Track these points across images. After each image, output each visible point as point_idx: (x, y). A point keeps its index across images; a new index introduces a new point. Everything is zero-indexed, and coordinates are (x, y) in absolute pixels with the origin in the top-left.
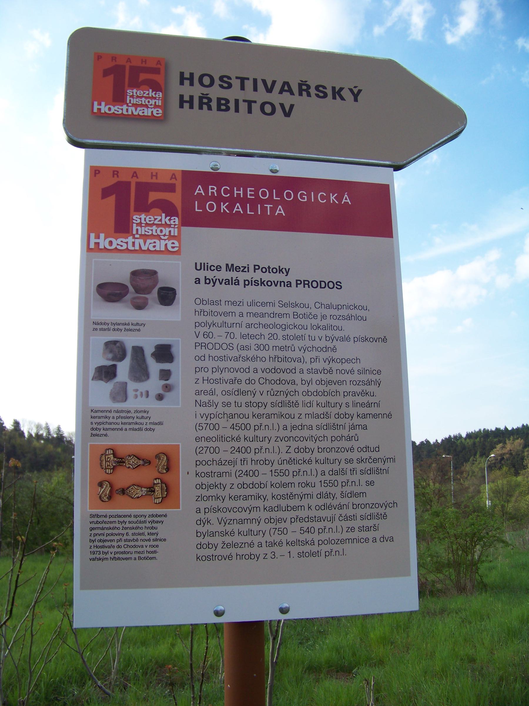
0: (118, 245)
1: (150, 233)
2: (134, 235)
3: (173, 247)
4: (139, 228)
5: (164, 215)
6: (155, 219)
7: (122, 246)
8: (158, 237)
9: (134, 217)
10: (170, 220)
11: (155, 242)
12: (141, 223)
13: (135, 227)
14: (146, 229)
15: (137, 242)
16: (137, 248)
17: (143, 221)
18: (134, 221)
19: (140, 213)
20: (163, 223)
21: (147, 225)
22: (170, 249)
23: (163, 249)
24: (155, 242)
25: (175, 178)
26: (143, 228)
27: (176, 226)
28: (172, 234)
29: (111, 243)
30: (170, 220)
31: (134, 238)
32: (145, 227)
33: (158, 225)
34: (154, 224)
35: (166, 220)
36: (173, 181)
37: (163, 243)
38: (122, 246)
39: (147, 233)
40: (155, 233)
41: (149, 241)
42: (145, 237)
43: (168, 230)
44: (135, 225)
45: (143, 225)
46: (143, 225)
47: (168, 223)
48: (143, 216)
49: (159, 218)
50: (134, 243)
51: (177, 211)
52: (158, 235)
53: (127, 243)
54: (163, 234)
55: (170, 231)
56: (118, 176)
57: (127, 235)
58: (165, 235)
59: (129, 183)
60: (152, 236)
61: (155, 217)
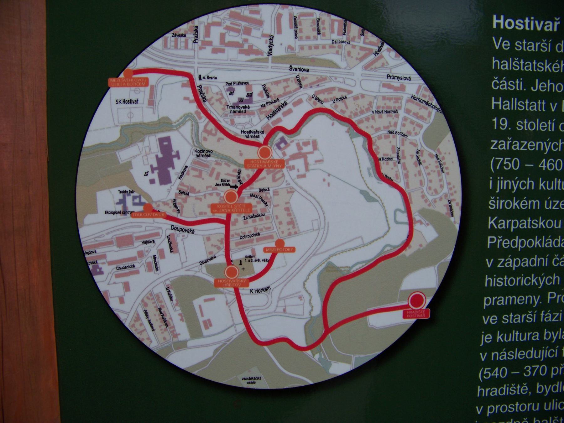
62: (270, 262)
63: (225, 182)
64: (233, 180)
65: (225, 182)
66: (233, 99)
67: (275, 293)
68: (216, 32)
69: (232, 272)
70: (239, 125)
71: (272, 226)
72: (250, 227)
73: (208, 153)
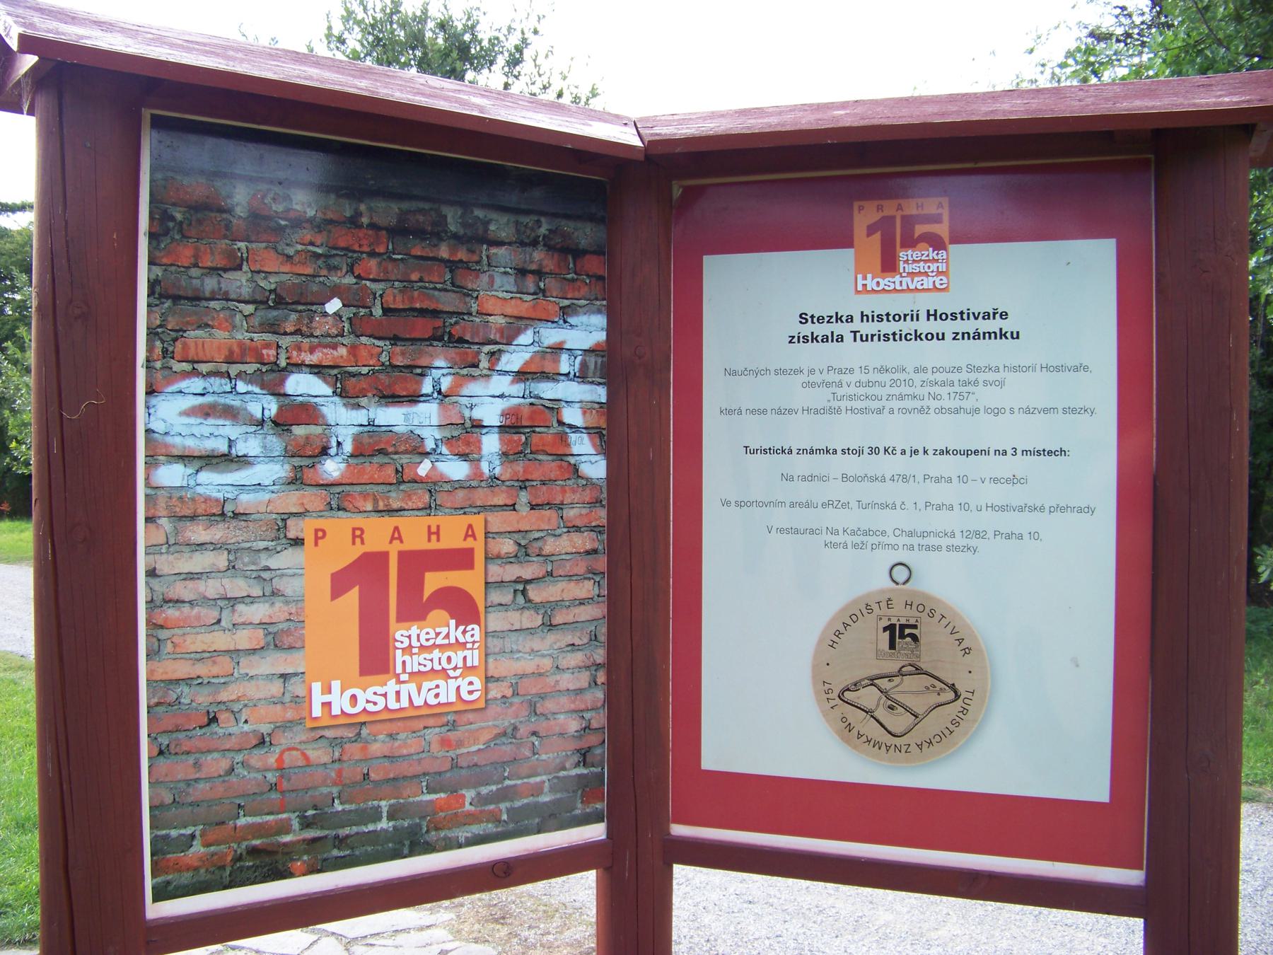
0: (368, 701)
3: (470, 692)
4: (407, 658)
5: (452, 623)
6: (438, 634)
7: (375, 704)
9: (398, 636)
10: (464, 632)
11: (437, 686)
12: (410, 646)
17: (415, 643)
18: (398, 645)
19: (407, 624)
23: (453, 698)
24: (437, 686)
25: (474, 536)
27: (476, 645)
28: (469, 664)
30: (464, 632)
31: (399, 682)
32: (419, 654)
34: (435, 646)
35: (456, 633)
36: (470, 543)
37: (453, 684)
38: (375, 704)
39: (422, 669)
40: (437, 667)
41: (426, 685)
43: (461, 654)
44: (399, 652)
47: (461, 640)
49: (444, 631)
50: (398, 693)
52: (444, 670)
53: (385, 695)
54: (453, 665)
55: (465, 658)
56: (363, 542)
58: (455, 668)
59: (385, 555)
61: (438, 630)
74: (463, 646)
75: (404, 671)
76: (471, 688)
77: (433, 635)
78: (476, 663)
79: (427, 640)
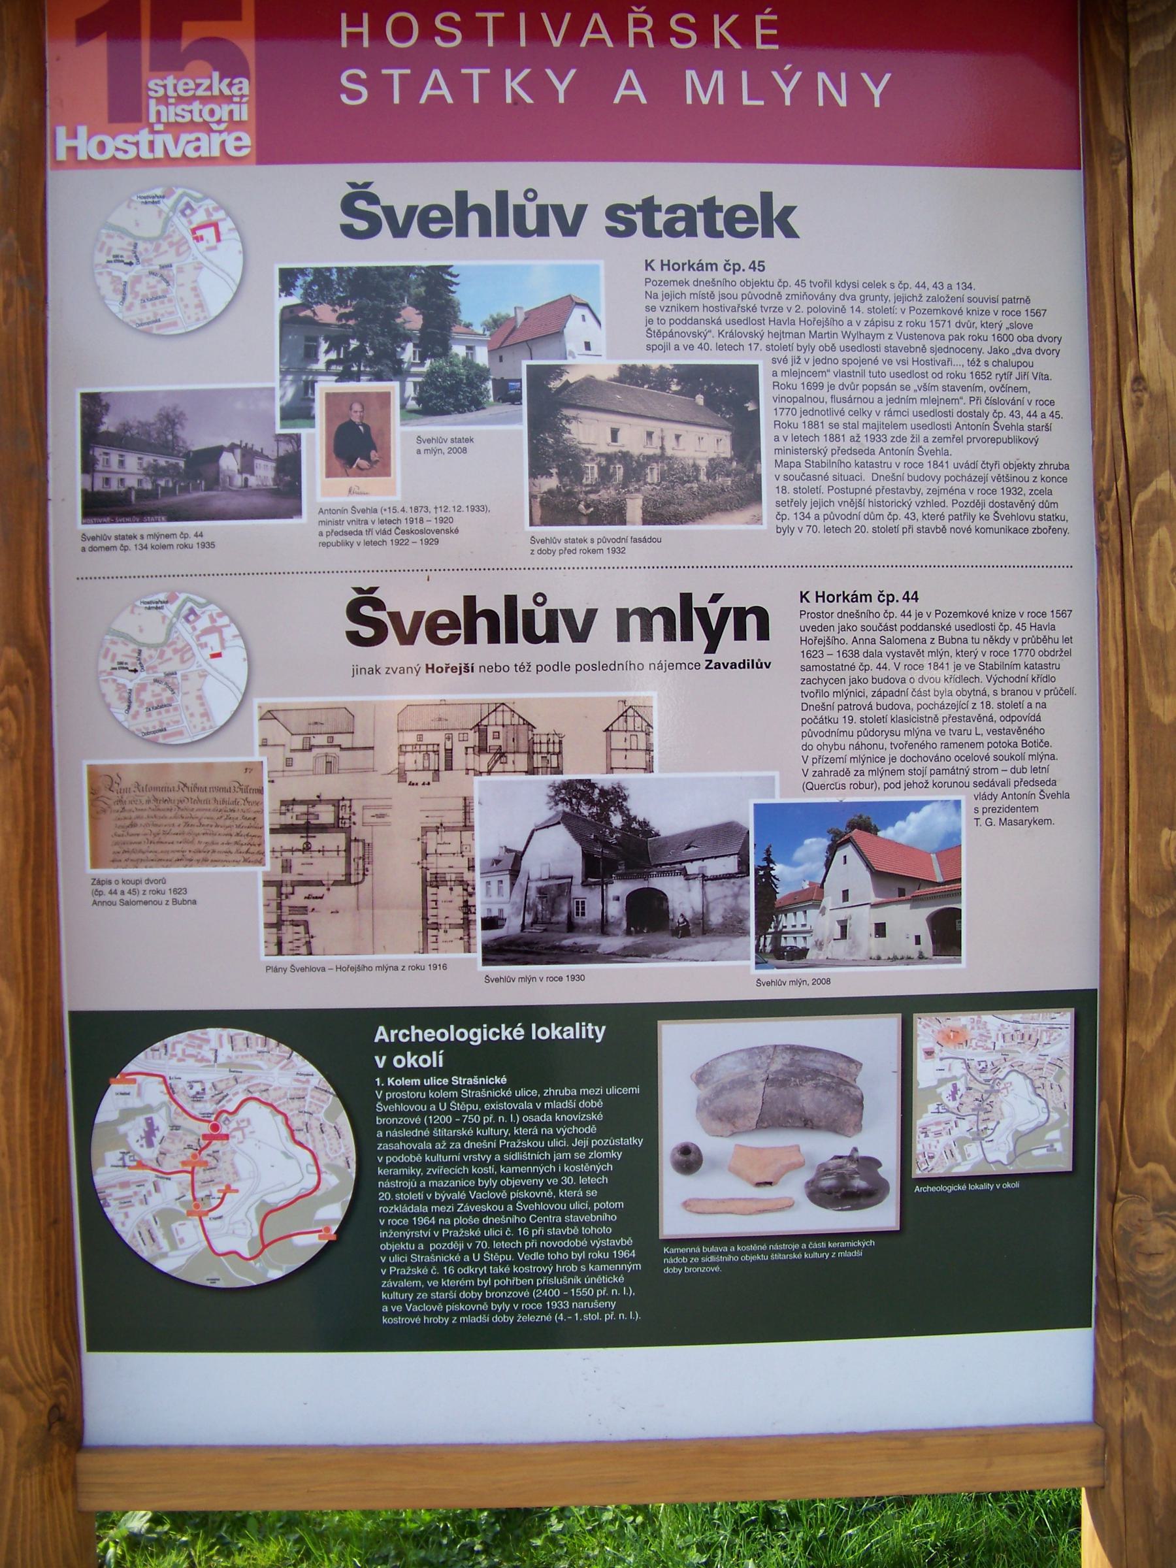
0: (117, 149)
1: (188, 118)
2: (151, 126)
4: (163, 109)
6: (198, 86)
7: (126, 152)
8: (206, 127)
9: (151, 85)
11: (198, 139)
12: (166, 96)
13: (153, 107)
14: (179, 110)
15: (159, 140)
16: (159, 154)
17: (171, 92)
18: (152, 94)
20: (216, 92)
21: (180, 100)
22: (232, 152)
24: (198, 139)
26: (172, 108)
28: (236, 118)
29: (102, 147)
31: (153, 132)
32: (176, 105)
33: (204, 100)
34: (195, 98)
35: (220, 86)
37: (216, 139)
38: (126, 152)
39: (180, 120)
40: (197, 119)
41: (184, 138)
42: (175, 128)
43: (226, 108)
44: (152, 102)
45: (172, 101)
46: (172, 101)
48: (170, 81)
50: (152, 144)
51: (243, 61)
52: (206, 123)
53: (137, 144)
54: (216, 118)
55: (231, 113)
57: (133, 126)
58: (219, 122)
60: (192, 126)
61: (198, 81)
62: (223, 1199)
63: (190, 1147)
64: (195, 1145)
65: (190, 1147)
66: (193, 1092)
67: (227, 1220)
68: (179, 1047)
69: (197, 1206)
70: (198, 1109)
71: (223, 1174)
72: (207, 1176)
73: (177, 1128)
74: (229, 99)
75: (159, 121)
76: (239, 144)
77: (192, 85)
78: (245, 117)
79: (186, 91)
